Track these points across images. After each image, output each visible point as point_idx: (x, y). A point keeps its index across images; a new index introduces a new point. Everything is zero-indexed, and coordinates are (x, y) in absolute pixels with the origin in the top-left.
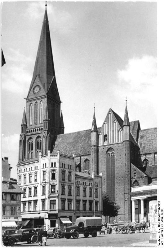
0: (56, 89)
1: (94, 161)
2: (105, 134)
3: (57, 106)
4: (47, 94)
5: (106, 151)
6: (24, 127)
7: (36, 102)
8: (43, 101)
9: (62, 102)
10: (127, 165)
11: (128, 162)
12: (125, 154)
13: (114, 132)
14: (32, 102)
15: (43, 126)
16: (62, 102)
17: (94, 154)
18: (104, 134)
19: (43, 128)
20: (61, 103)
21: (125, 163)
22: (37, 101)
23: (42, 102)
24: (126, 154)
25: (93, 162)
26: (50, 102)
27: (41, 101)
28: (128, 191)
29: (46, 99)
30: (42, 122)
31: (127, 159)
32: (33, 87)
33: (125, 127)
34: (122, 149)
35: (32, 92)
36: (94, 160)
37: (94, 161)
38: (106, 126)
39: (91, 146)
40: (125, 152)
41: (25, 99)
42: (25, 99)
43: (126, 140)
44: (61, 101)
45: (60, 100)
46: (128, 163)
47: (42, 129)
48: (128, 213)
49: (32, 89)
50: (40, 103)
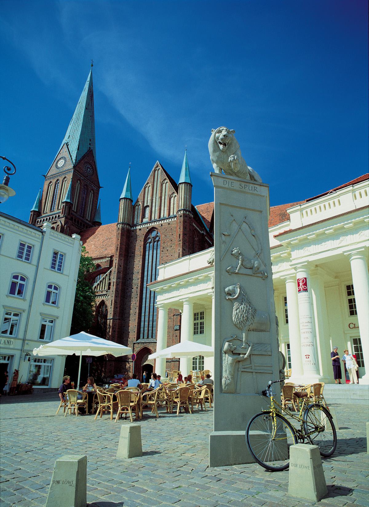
2: (145, 205)
4: (74, 167)
5: (145, 234)
6: (34, 214)
7: (58, 180)
9: (102, 187)
11: (184, 250)
12: (178, 235)
14: (51, 180)
15: (60, 213)
16: (102, 187)
19: (60, 214)
20: (101, 189)
21: (178, 252)
22: (58, 178)
24: (180, 235)
27: (65, 177)
29: (72, 174)
34: (175, 230)
40: (179, 230)
44: (101, 186)
45: (99, 186)
47: (59, 215)
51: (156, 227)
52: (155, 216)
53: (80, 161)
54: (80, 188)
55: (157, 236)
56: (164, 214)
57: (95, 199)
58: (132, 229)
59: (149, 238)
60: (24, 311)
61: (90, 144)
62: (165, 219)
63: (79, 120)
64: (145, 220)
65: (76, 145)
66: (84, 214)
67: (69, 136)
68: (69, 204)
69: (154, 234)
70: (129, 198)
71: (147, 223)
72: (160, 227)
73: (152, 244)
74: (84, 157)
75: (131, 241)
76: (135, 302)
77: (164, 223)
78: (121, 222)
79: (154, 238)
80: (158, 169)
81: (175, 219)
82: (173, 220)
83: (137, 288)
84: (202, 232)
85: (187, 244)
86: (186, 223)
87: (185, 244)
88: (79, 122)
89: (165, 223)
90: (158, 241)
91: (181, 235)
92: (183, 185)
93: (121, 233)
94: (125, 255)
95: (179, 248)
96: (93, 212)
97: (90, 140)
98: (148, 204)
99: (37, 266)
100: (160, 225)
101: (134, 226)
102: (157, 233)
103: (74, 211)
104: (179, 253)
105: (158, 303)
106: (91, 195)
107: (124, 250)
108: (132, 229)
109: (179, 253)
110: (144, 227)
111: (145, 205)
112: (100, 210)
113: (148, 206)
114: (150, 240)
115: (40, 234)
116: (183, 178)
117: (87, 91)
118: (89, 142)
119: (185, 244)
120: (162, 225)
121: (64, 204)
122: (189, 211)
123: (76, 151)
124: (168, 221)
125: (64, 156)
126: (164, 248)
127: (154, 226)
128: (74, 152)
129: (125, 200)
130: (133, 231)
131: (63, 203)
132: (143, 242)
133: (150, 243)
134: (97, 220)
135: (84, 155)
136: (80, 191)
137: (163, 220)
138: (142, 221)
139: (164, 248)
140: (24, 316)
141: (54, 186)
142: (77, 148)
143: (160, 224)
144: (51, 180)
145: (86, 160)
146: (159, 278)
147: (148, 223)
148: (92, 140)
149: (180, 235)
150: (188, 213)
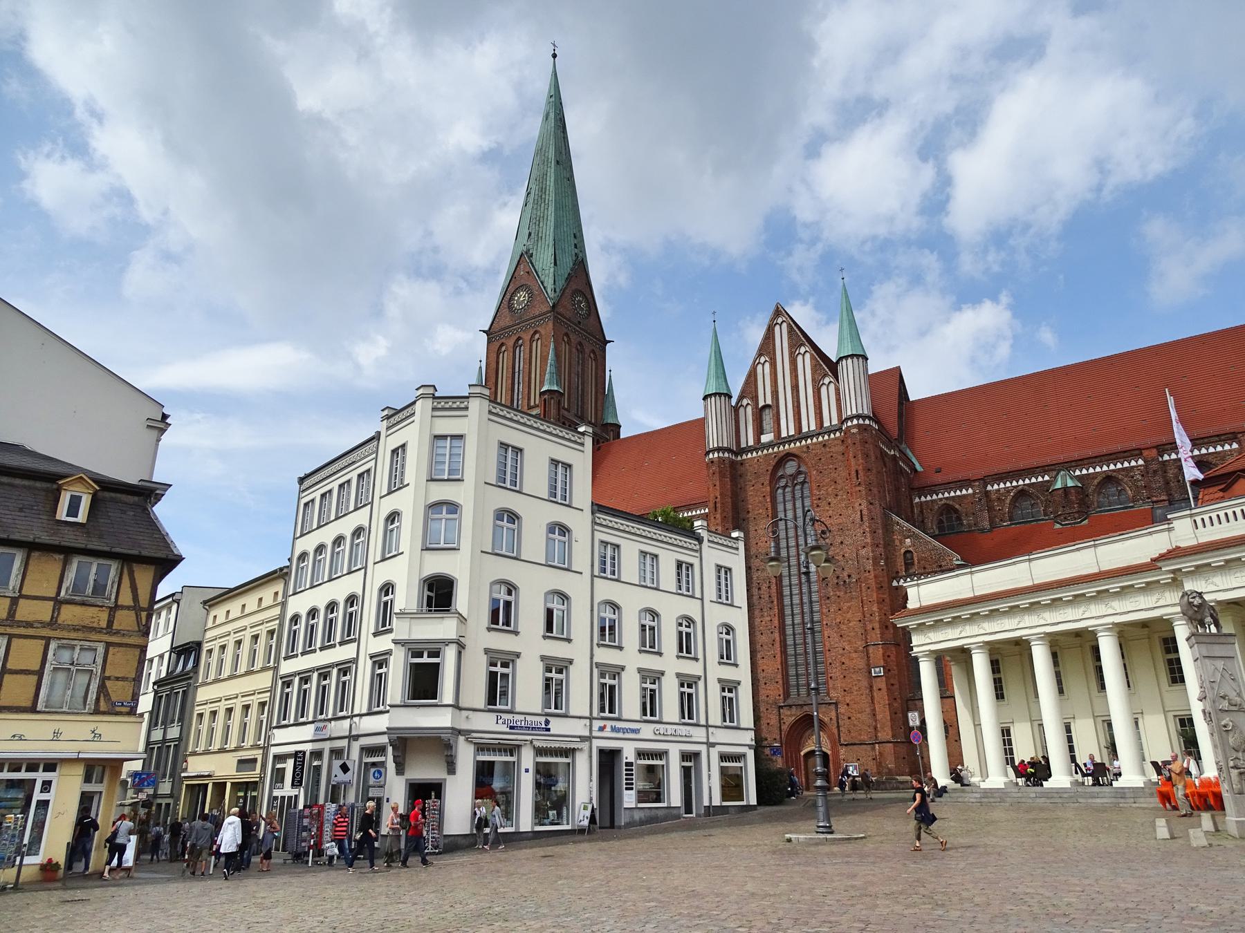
0: (589, 297)
1: (719, 510)
2: (761, 404)
3: (593, 352)
5: (770, 468)
8: (543, 332)
9: (610, 342)
10: (865, 518)
11: (871, 504)
13: (798, 391)
16: (610, 342)
17: (718, 483)
18: (757, 403)
21: (858, 508)
23: (537, 336)
24: (857, 471)
25: (718, 516)
26: (567, 334)
27: (536, 332)
28: (882, 634)
29: (551, 324)
30: (537, 402)
31: (864, 492)
32: (511, 289)
33: (844, 361)
34: (840, 457)
35: (505, 311)
36: (718, 505)
37: (719, 510)
38: (764, 371)
39: (708, 453)
40: (853, 461)
41: (484, 331)
42: (484, 331)
43: (854, 412)
44: (607, 339)
46: (870, 511)
48: (893, 736)
49: (508, 296)
50: (531, 341)
51: (797, 453)
52: (787, 429)
53: (563, 291)
54: (570, 351)
55: (799, 473)
56: (808, 424)
57: (599, 372)
58: (739, 458)
59: (782, 477)
60: (699, 678)
61: (576, 246)
62: (813, 436)
63: (545, 193)
64: (766, 438)
65: (550, 254)
66: (582, 412)
67: (530, 234)
68: (557, 394)
69: (791, 468)
70: (725, 392)
71: (770, 445)
72: (805, 452)
73: (788, 489)
74: (569, 278)
75: (739, 486)
76: (769, 619)
77: (812, 444)
78: (716, 446)
79: (794, 477)
80: (780, 320)
81: (838, 434)
82: (832, 436)
83: (769, 587)
84: (892, 453)
85: (875, 490)
86: (867, 446)
87: (870, 490)
88: (547, 197)
89: (815, 444)
90: (803, 483)
91: (860, 472)
92: (850, 360)
93: (720, 472)
94: (733, 518)
95: (859, 501)
96: (599, 403)
97: (575, 237)
98: (769, 402)
99: (702, 599)
100: (805, 449)
101: (744, 452)
102: (799, 467)
103: (564, 408)
104: (861, 511)
105: (915, 650)
106: (591, 365)
107: (730, 507)
108: (739, 458)
109: (861, 511)
110: (766, 455)
111: (761, 404)
112: (613, 396)
113: (766, 406)
114: (783, 483)
115: (696, 543)
116: (846, 345)
117: (553, 121)
118: (573, 241)
119: (870, 490)
120: (808, 447)
121: (546, 396)
122: (869, 418)
123: (552, 270)
124: (820, 439)
125: (523, 282)
126: (819, 499)
127: (791, 451)
128: (547, 272)
129: (717, 397)
130: (742, 464)
131: (542, 394)
132: (768, 488)
133: (785, 487)
134: (610, 421)
135: (569, 274)
136: (570, 359)
137: (808, 437)
138: (759, 439)
139: (819, 499)
140: (701, 684)
141: (511, 354)
142: (553, 261)
143: (803, 446)
144: (503, 341)
145: (574, 287)
146: (912, 604)
147: (775, 445)
148: (578, 235)
149: (857, 471)
150: (867, 422)
